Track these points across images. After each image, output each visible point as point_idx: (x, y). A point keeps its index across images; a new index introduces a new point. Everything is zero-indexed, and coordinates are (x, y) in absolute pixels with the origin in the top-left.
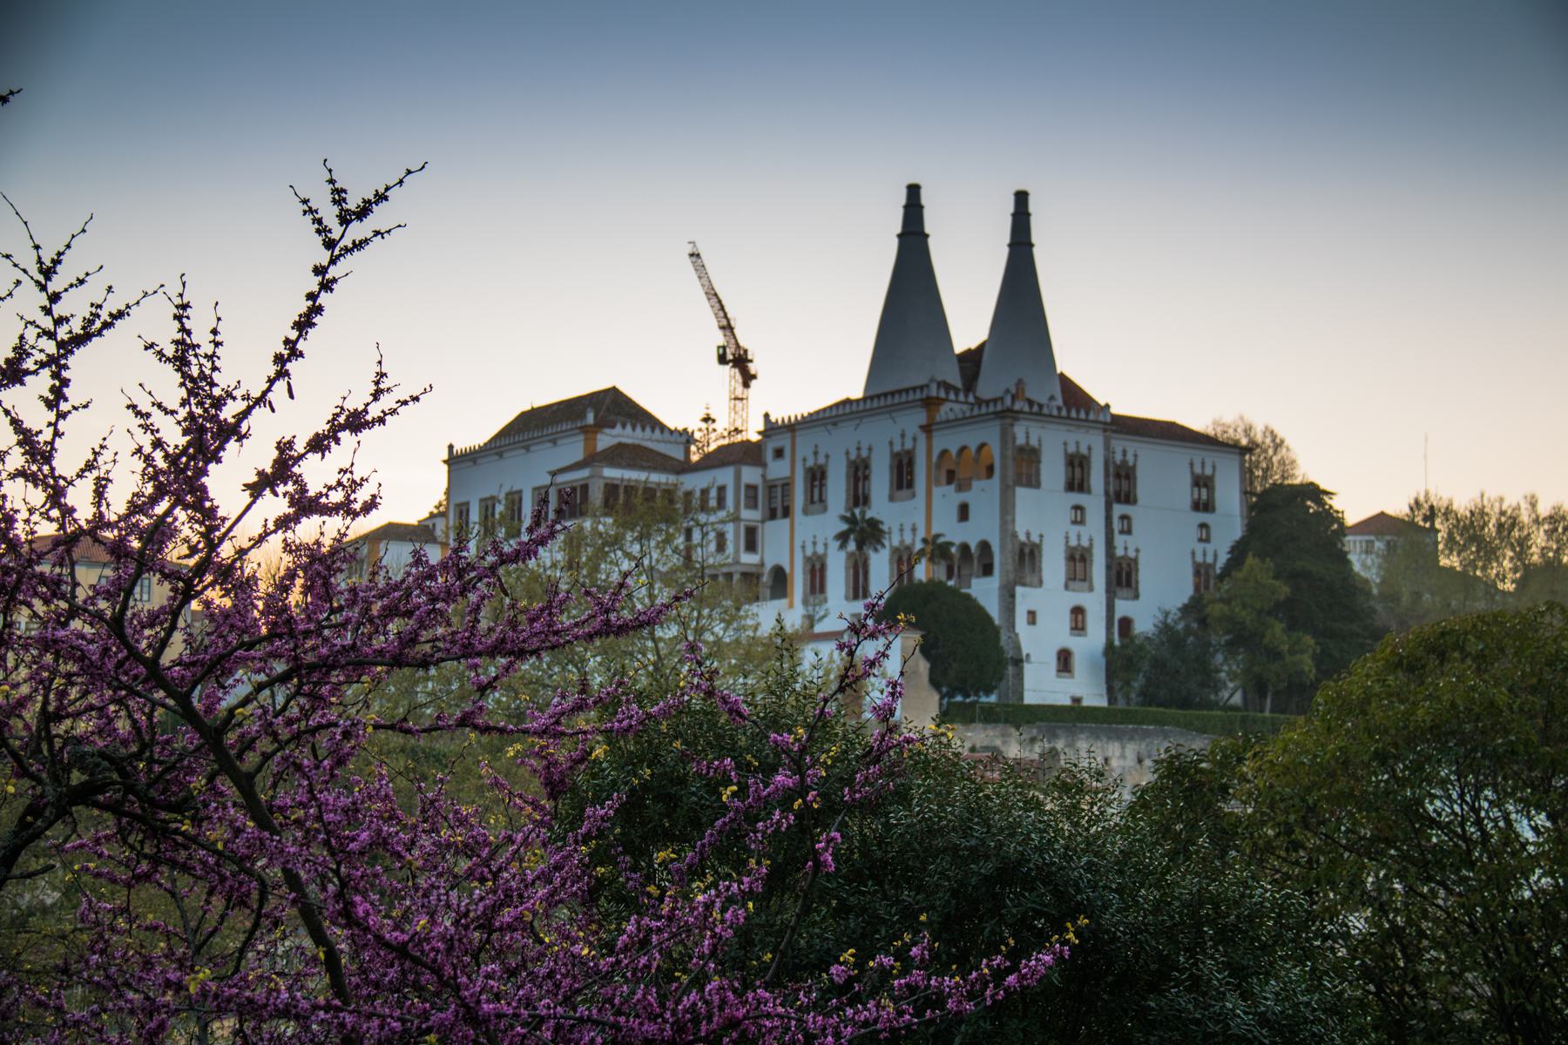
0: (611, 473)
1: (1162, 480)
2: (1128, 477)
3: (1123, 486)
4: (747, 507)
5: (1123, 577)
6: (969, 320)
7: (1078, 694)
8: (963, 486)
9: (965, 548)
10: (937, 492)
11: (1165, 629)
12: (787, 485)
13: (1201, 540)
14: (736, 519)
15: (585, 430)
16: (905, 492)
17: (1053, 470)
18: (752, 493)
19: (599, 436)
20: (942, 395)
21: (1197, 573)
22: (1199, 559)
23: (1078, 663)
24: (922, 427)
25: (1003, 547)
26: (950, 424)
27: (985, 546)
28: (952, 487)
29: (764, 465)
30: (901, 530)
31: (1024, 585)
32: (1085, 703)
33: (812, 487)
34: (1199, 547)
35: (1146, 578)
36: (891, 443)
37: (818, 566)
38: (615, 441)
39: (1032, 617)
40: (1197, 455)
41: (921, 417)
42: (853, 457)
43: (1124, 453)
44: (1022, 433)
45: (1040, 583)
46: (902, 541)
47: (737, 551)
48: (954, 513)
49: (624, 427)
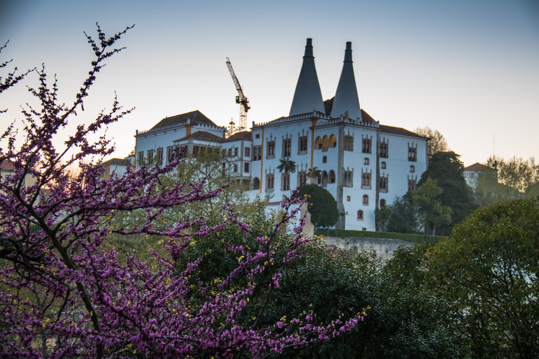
0: (196, 142)
1: (398, 148)
2: (385, 148)
3: (383, 151)
4: (246, 156)
5: (382, 184)
6: (328, 90)
7: (365, 226)
8: (325, 150)
9: (325, 172)
10: (315, 152)
11: (397, 204)
12: (260, 148)
13: (411, 172)
14: (241, 160)
15: (187, 126)
16: (303, 152)
17: (358, 145)
18: (247, 151)
19: (192, 128)
20: (318, 116)
21: (409, 184)
22: (410, 178)
23: (365, 215)
24: (310, 128)
25: (339, 173)
26: (320, 127)
27: (332, 172)
28: (321, 150)
29: (252, 141)
30: (302, 165)
31: (346, 186)
32: (367, 230)
33: (270, 149)
34: (410, 174)
35: (391, 185)
36: (299, 134)
37: (271, 178)
38: (198, 130)
39: (349, 198)
40: (411, 140)
41: (310, 124)
42: (285, 138)
43: (384, 139)
44: (347, 131)
45: (352, 186)
46: (302, 170)
47: (242, 171)
48: (321, 160)
49: (201, 125)
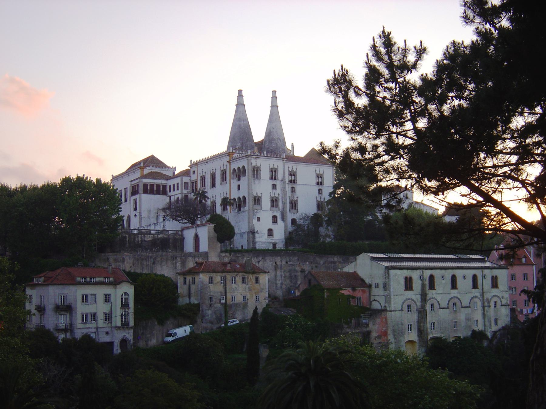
0: (146, 181)
5: (294, 205)
15: (141, 168)
17: (265, 174)
18: (186, 185)
19: (145, 170)
22: (319, 200)
23: (275, 233)
25: (249, 197)
38: (150, 171)
39: (259, 219)
41: (228, 159)
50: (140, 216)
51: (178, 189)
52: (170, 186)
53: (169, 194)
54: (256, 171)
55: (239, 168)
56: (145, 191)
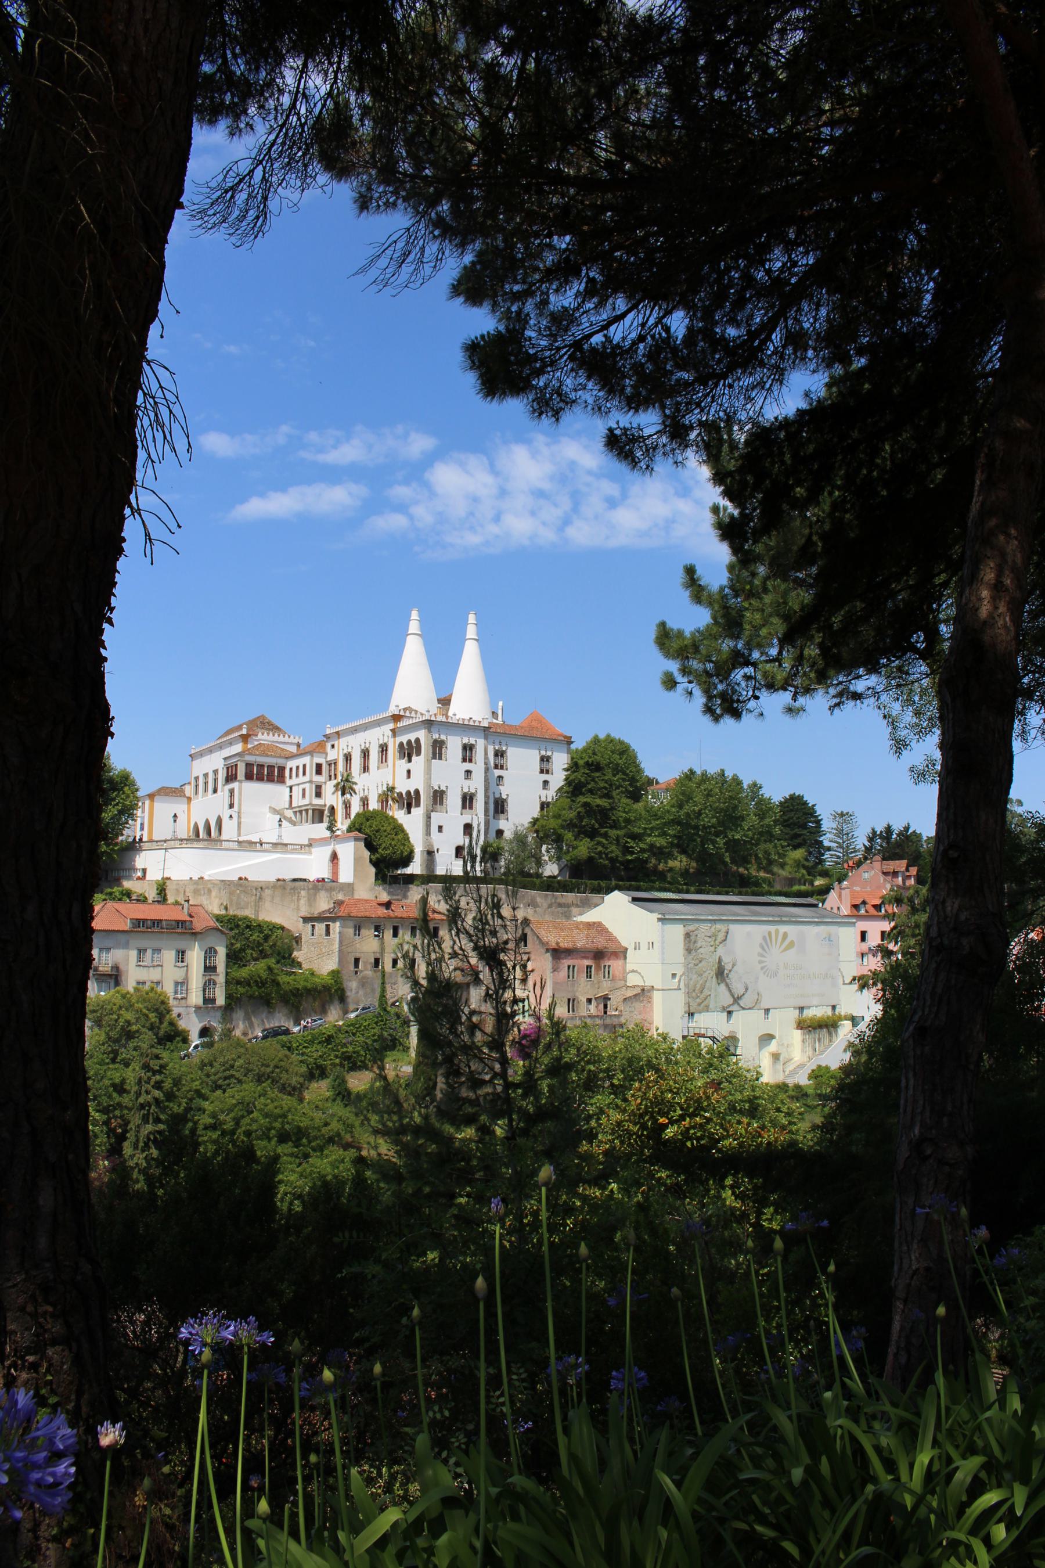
5: (499, 807)
9: (408, 793)
20: (402, 713)
21: (542, 808)
29: (327, 754)
34: (544, 793)
35: (511, 807)
39: (440, 828)
41: (391, 726)
48: (405, 773)
50: (239, 817)
51: (304, 774)
52: (291, 769)
53: (289, 782)
54: (438, 749)
55: (409, 742)
56: (249, 777)
